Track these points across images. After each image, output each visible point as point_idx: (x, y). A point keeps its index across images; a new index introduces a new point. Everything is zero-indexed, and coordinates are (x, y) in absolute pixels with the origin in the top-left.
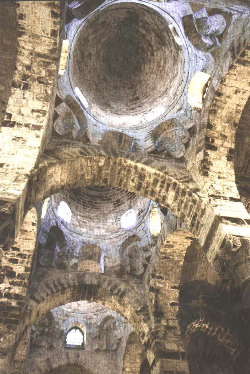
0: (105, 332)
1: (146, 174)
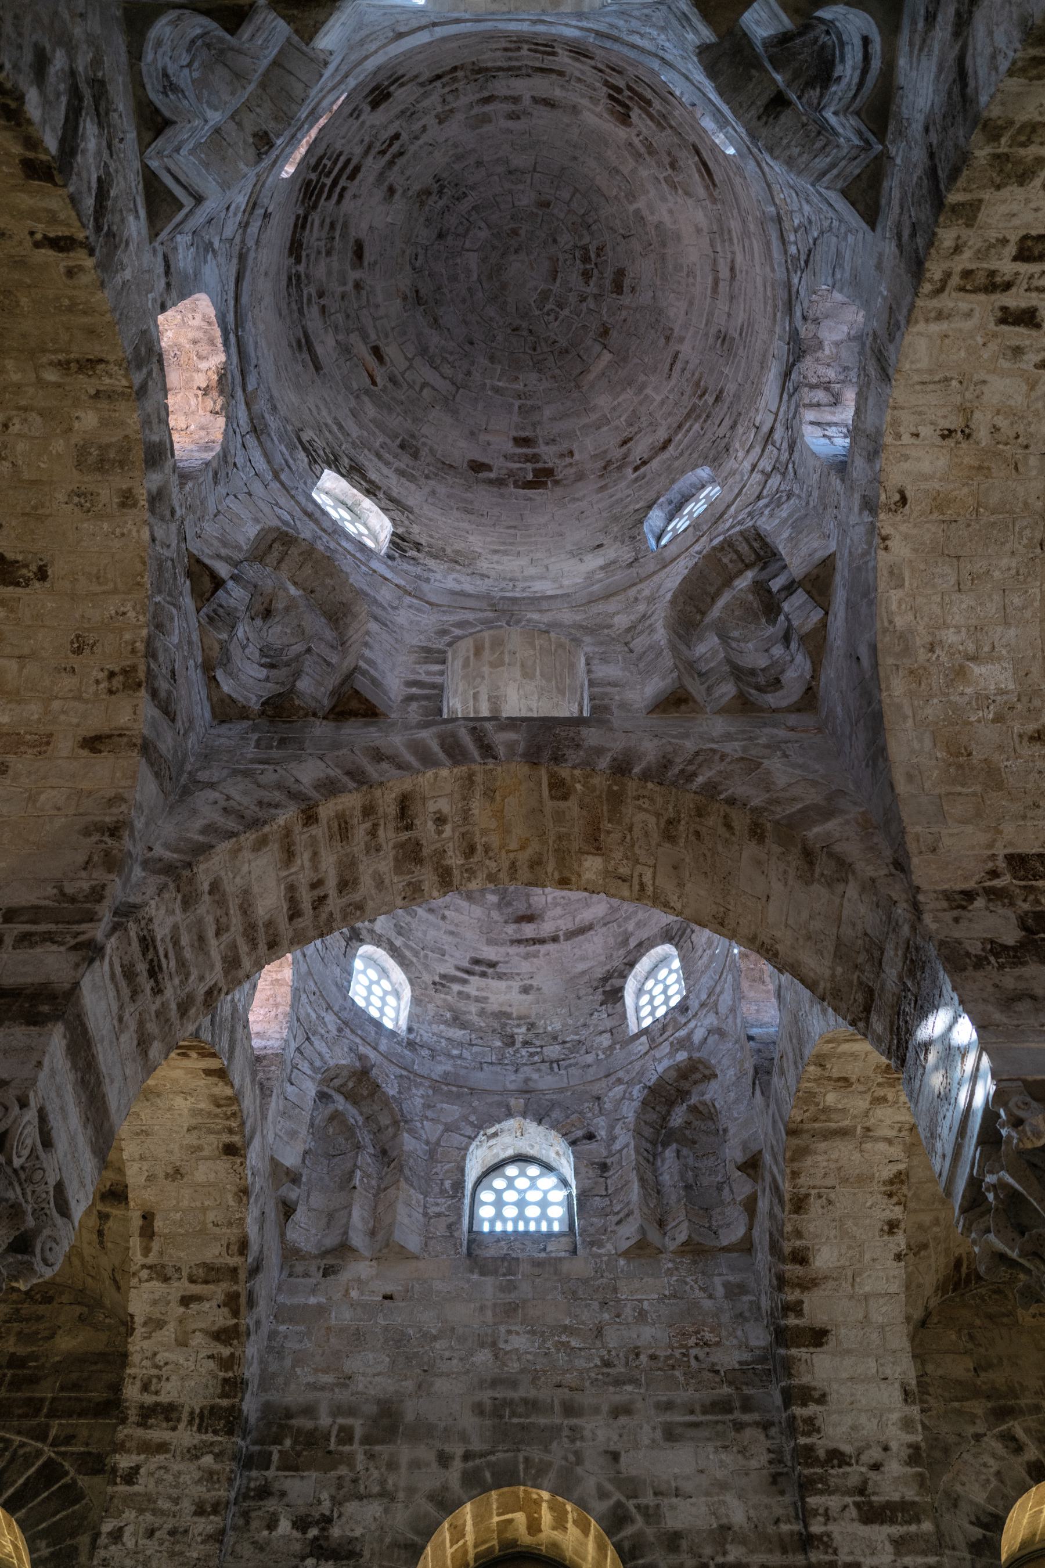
1: (395, 879)
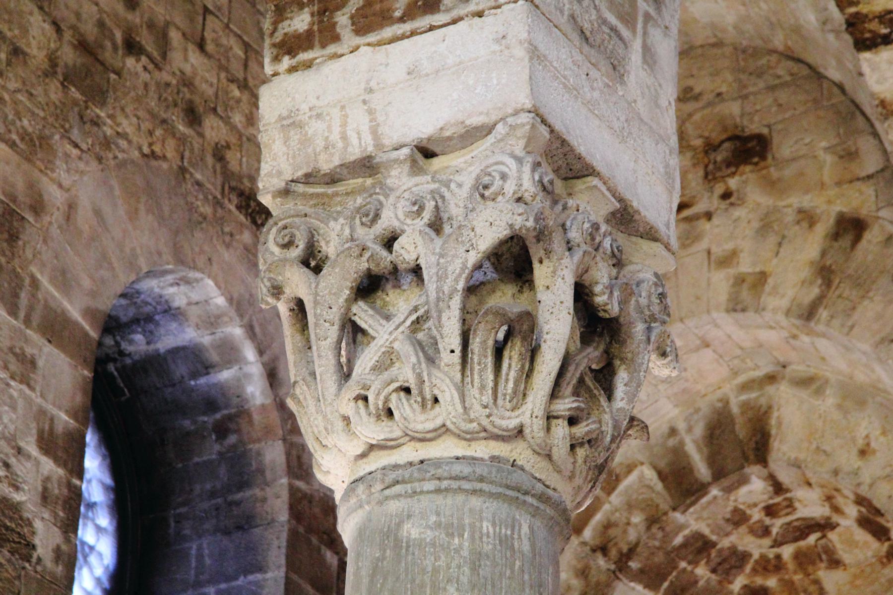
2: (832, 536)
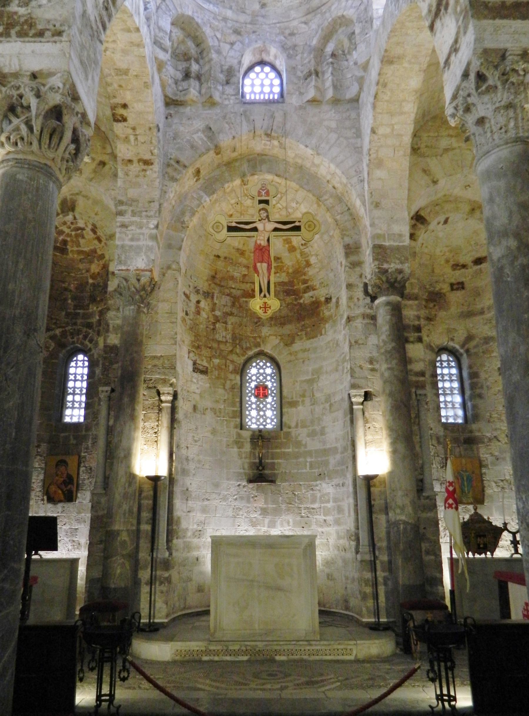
0: (331, 60)
2: (84, 232)
